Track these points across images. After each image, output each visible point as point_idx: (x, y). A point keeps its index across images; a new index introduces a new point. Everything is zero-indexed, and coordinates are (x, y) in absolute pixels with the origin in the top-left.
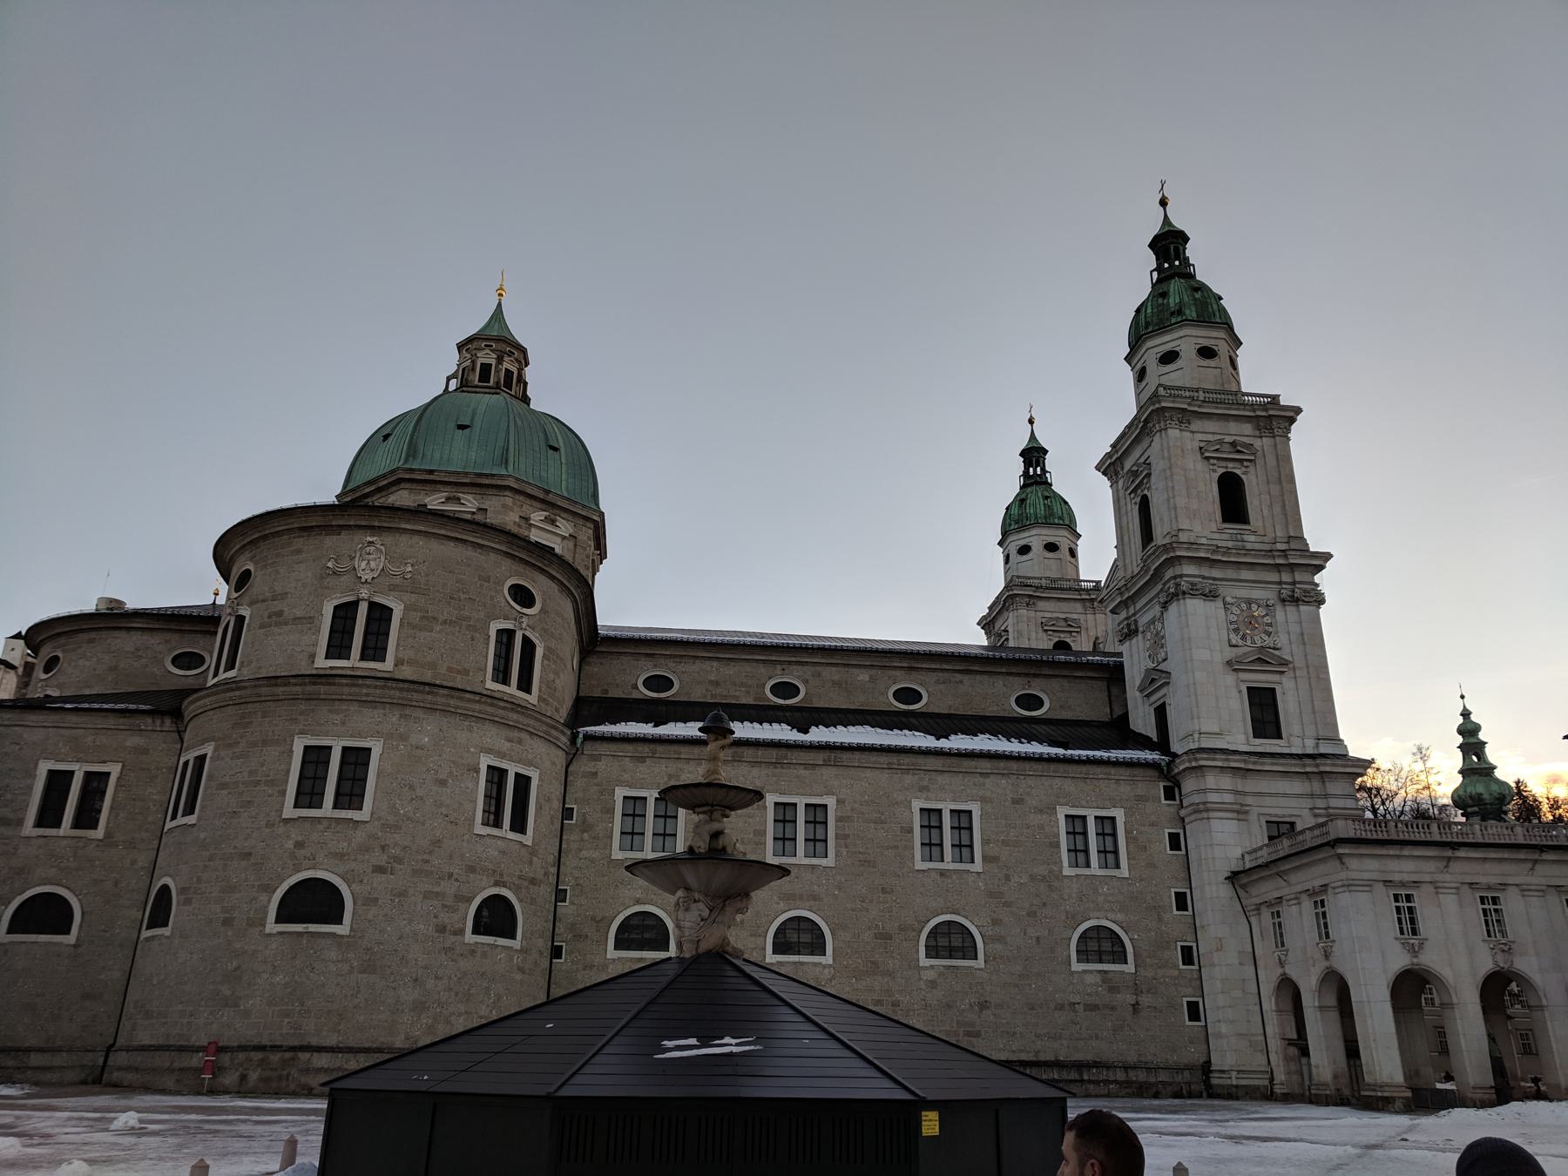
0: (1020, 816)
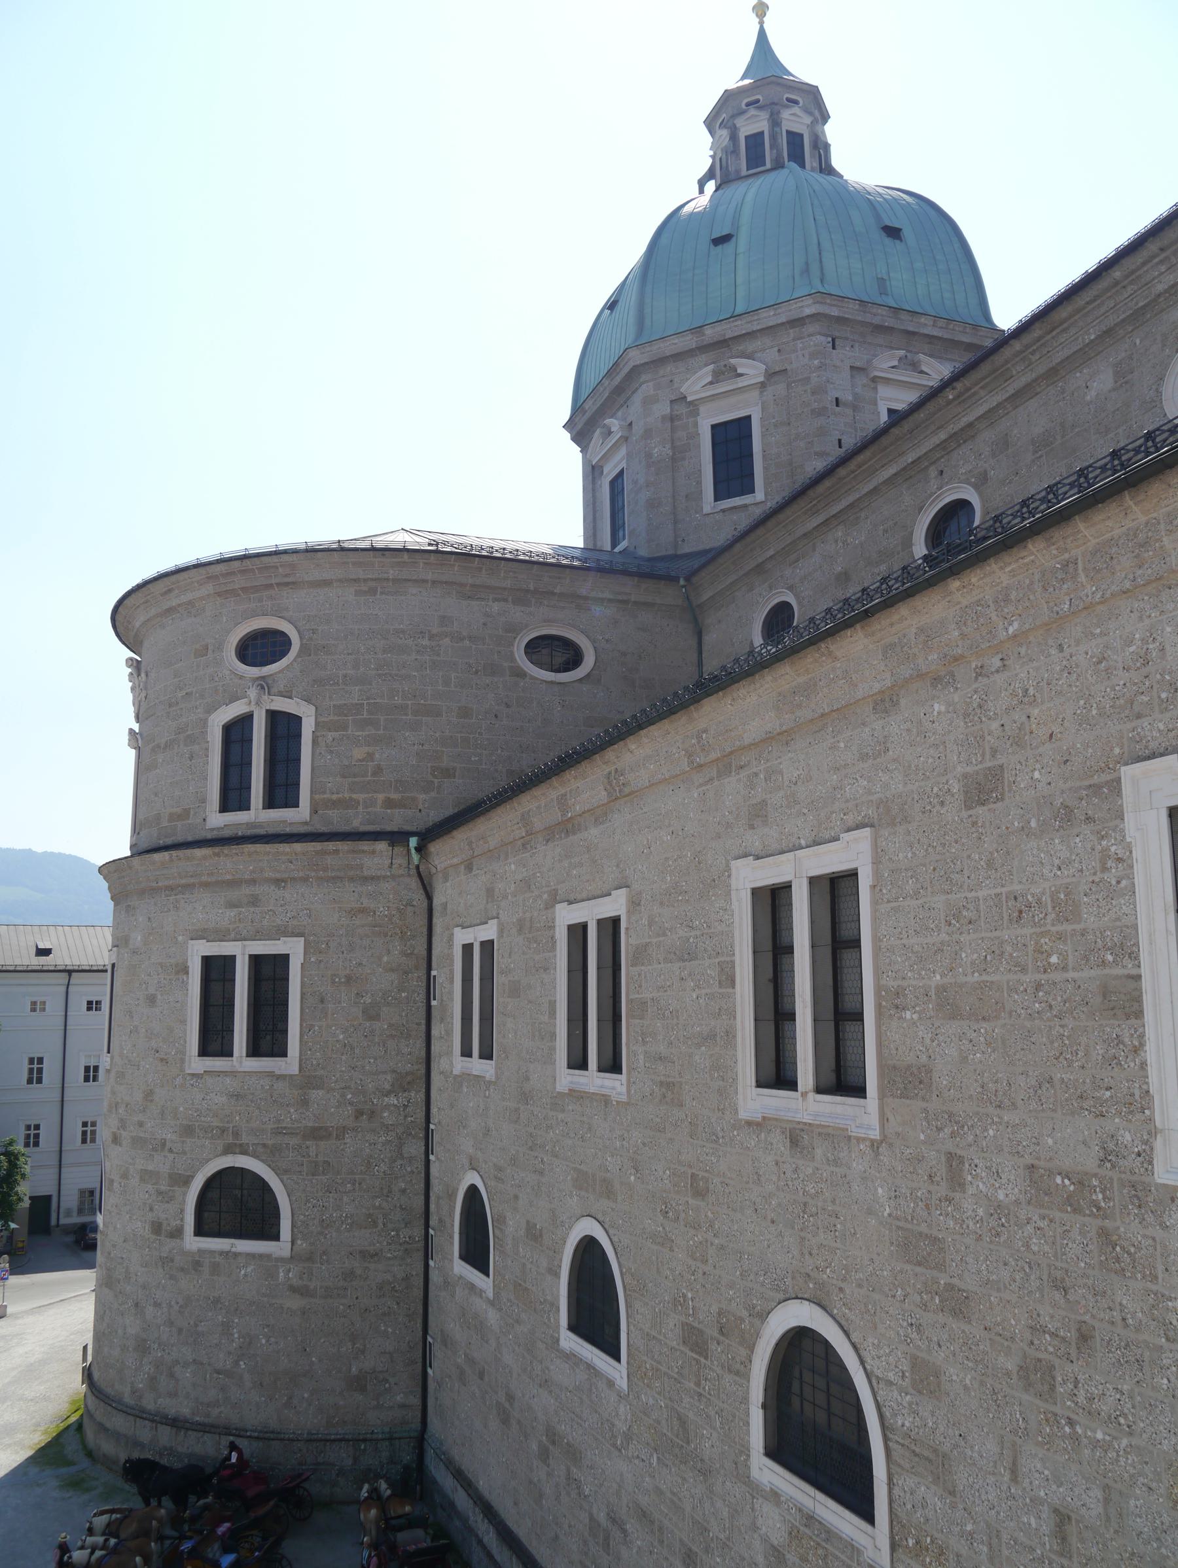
0: (990, 864)
